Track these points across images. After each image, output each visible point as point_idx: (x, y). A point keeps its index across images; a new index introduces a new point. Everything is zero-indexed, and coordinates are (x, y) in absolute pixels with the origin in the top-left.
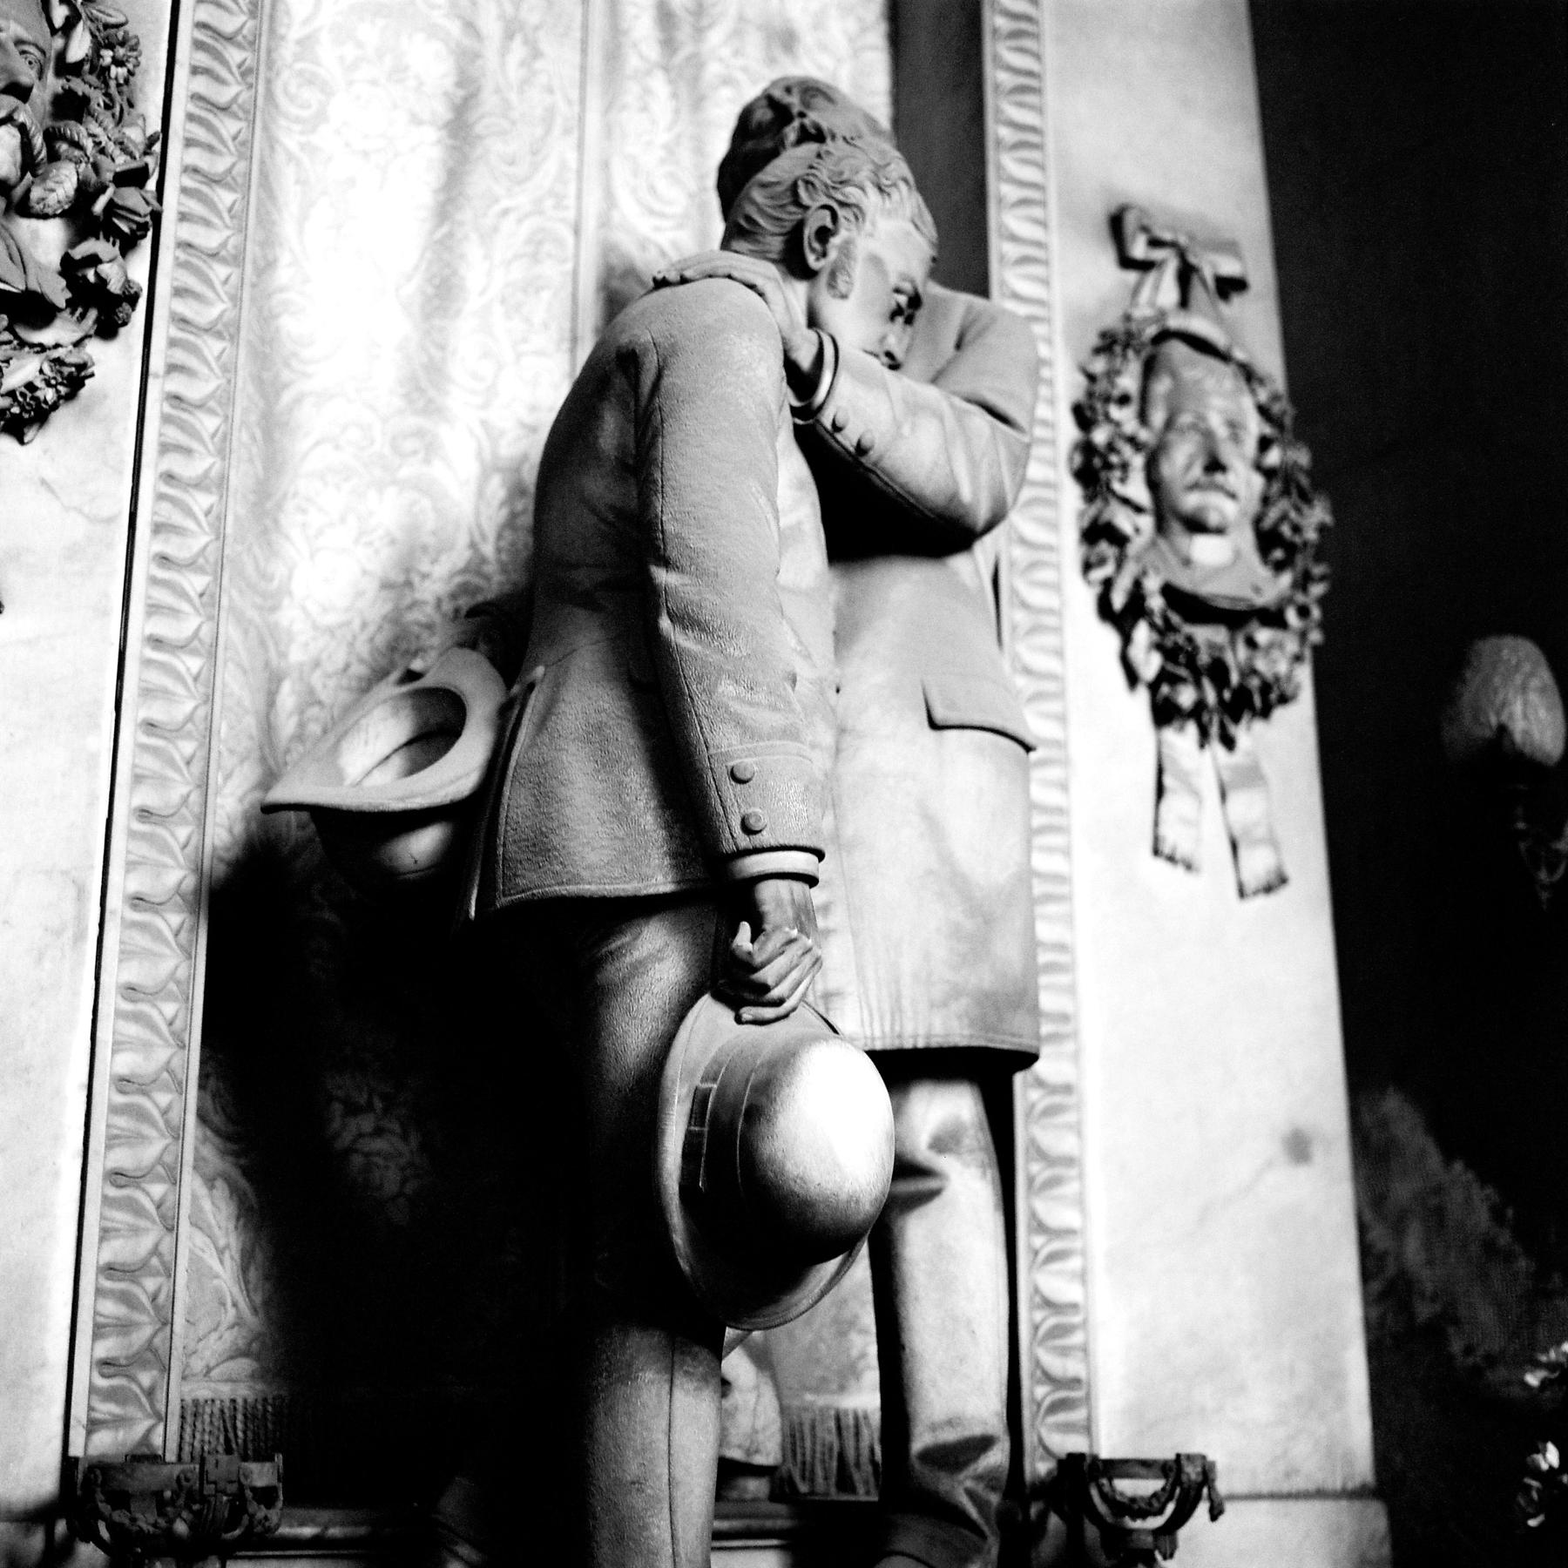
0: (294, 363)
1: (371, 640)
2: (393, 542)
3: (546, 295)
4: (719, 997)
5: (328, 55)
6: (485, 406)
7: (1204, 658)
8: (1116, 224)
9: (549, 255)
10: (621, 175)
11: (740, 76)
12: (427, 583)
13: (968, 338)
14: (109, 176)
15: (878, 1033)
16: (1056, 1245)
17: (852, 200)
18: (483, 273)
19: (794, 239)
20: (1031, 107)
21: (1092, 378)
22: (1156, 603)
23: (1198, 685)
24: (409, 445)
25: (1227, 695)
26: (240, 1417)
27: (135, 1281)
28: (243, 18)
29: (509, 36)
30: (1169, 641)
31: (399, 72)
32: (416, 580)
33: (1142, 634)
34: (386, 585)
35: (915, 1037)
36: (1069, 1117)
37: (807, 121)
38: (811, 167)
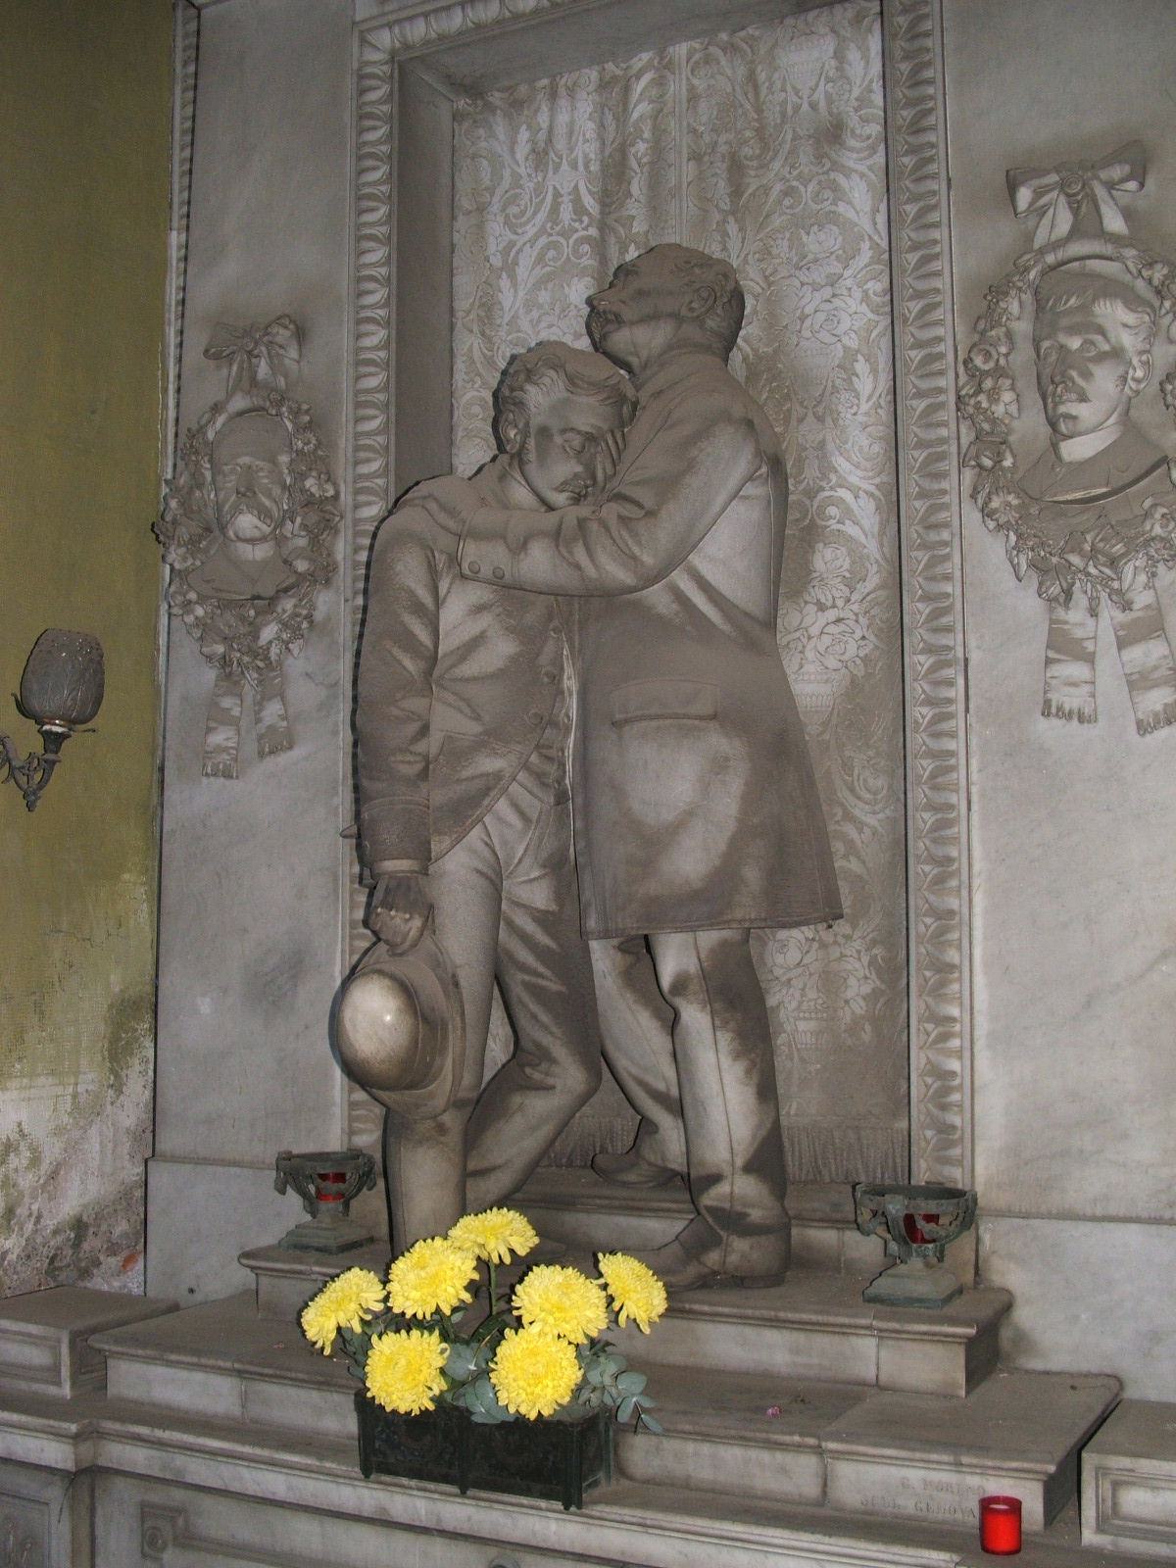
11: (795, 183)
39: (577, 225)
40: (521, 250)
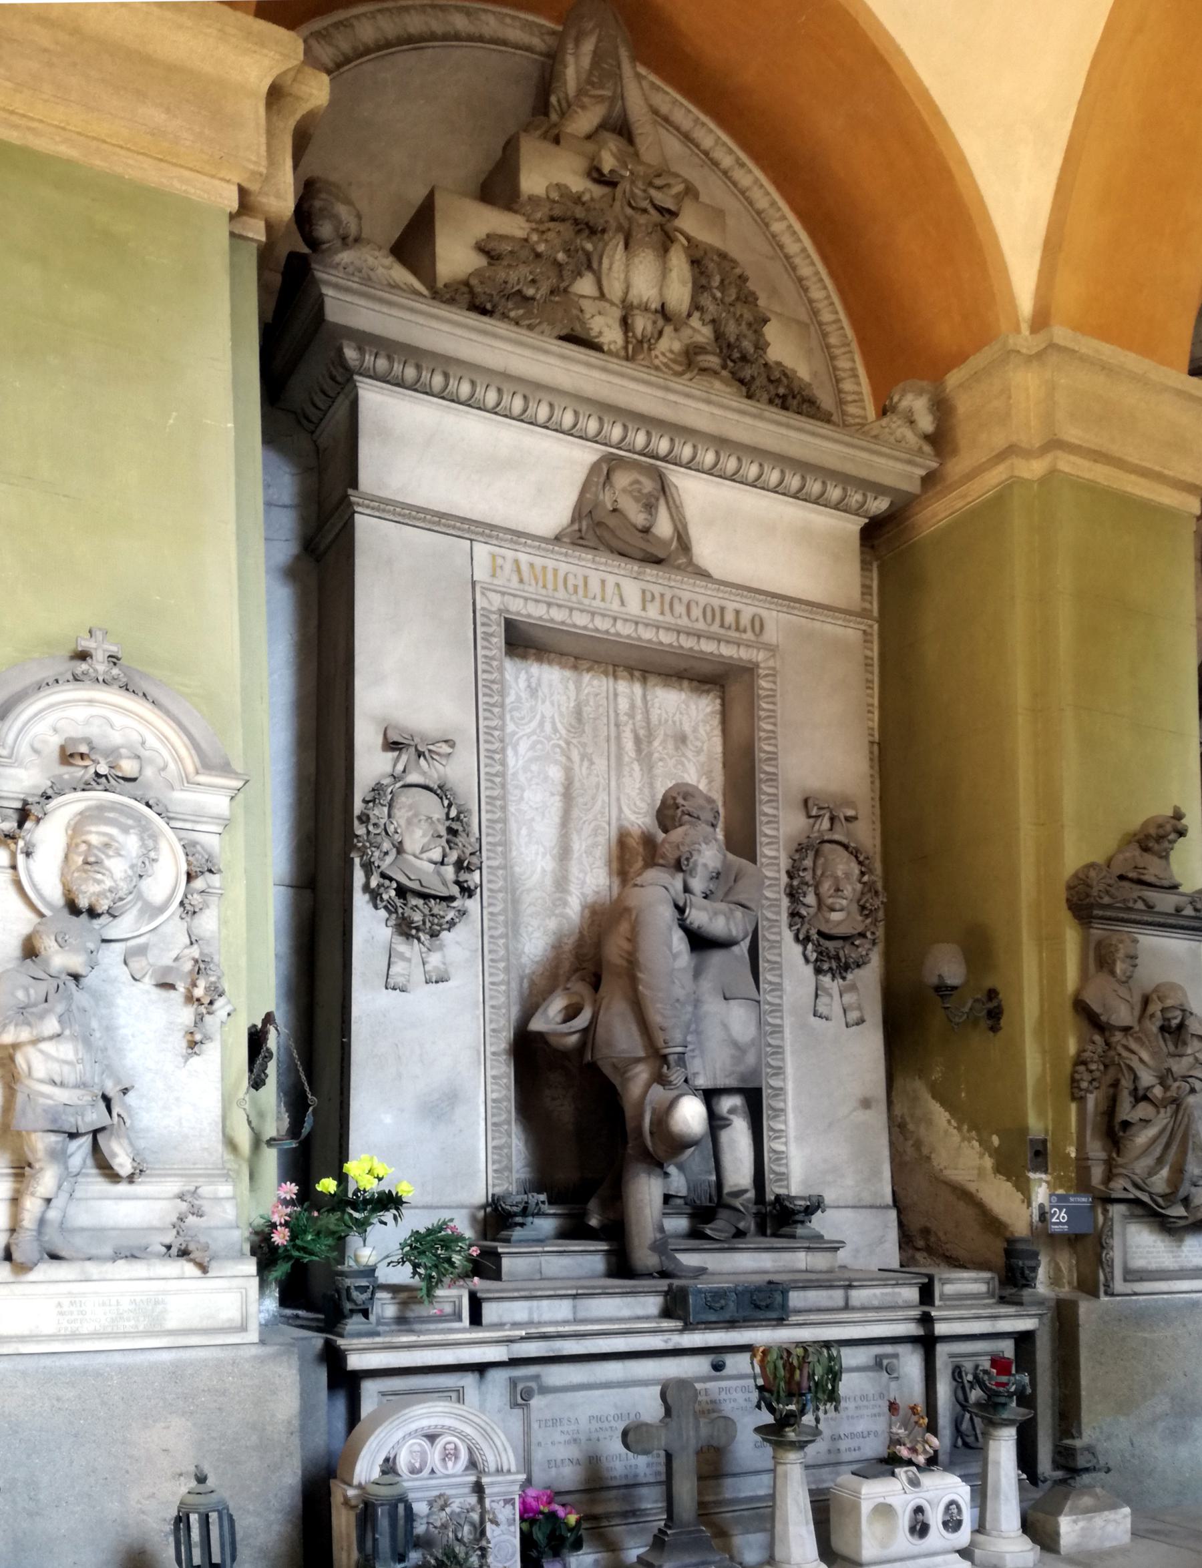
5: (522, 778)
7: (833, 953)
18: (578, 845)
22: (815, 937)
29: (582, 760)
30: (820, 949)
31: (546, 778)
33: (810, 946)
40: (520, 738)
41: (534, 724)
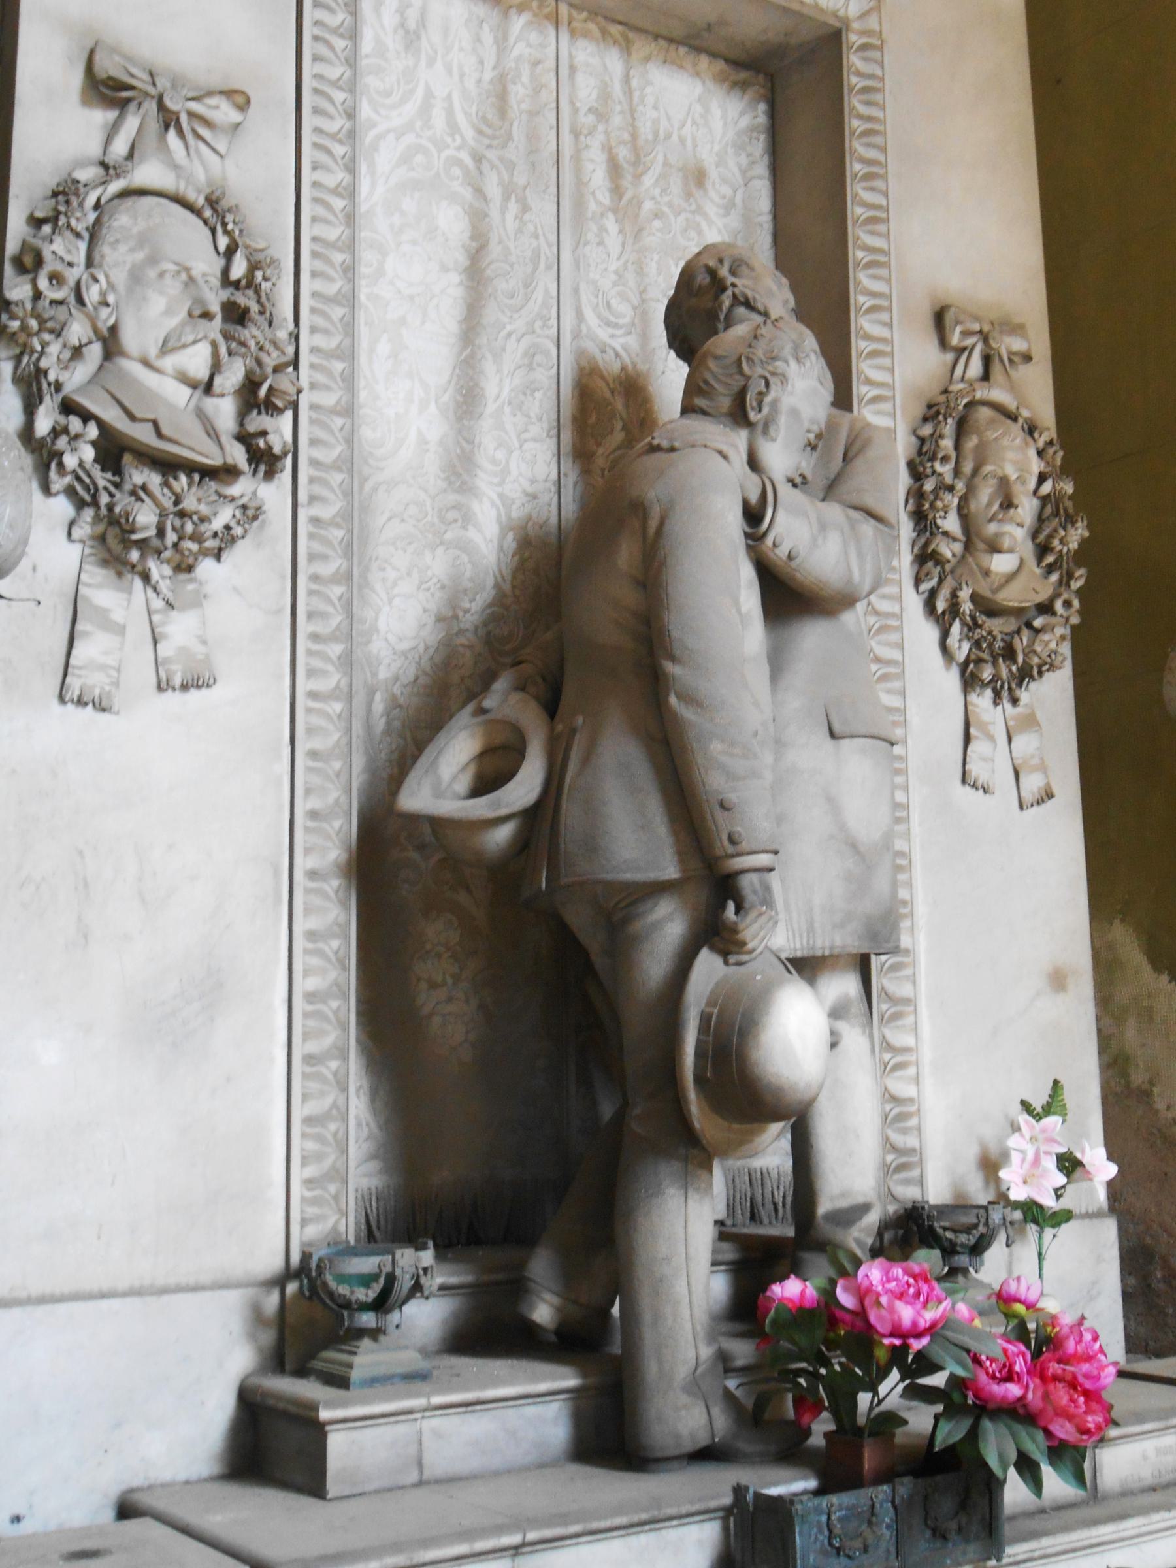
0: (371, 461)
1: (431, 658)
2: (443, 587)
3: (538, 395)
4: (713, 948)
6: (502, 483)
8: (939, 318)
9: (539, 365)
10: (586, 297)
11: (665, 209)
12: (468, 616)
13: (850, 454)
14: (269, 370)
15: (798, 946)
16: (899, 1059)
17: (779, 371)
18: (498, 385)
19: (740, 398)
20: (879, 235)
21: (922, 441)
22: (967, 607)
23: (995, 664)
24: (451, 515)
25: (1014, 668)
26: (374, 1198)
27: (323, 1126)
28: (342, 228)
29: (506, 198)
32: (461, 614)
33: (956, 628)
34: (440, 619)
35: (823, 948)
36: (908, 972)
37: (736, 290)
38: (750, 346)
39: (449, 140)
40: (380, 137)
41: (411, 108)
